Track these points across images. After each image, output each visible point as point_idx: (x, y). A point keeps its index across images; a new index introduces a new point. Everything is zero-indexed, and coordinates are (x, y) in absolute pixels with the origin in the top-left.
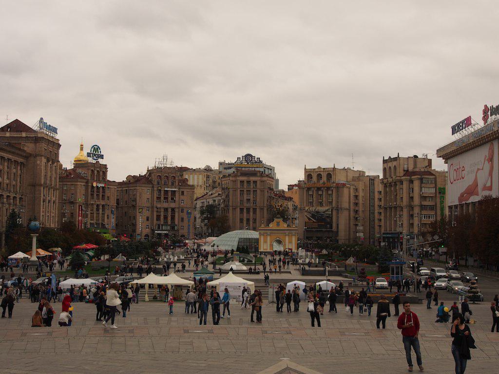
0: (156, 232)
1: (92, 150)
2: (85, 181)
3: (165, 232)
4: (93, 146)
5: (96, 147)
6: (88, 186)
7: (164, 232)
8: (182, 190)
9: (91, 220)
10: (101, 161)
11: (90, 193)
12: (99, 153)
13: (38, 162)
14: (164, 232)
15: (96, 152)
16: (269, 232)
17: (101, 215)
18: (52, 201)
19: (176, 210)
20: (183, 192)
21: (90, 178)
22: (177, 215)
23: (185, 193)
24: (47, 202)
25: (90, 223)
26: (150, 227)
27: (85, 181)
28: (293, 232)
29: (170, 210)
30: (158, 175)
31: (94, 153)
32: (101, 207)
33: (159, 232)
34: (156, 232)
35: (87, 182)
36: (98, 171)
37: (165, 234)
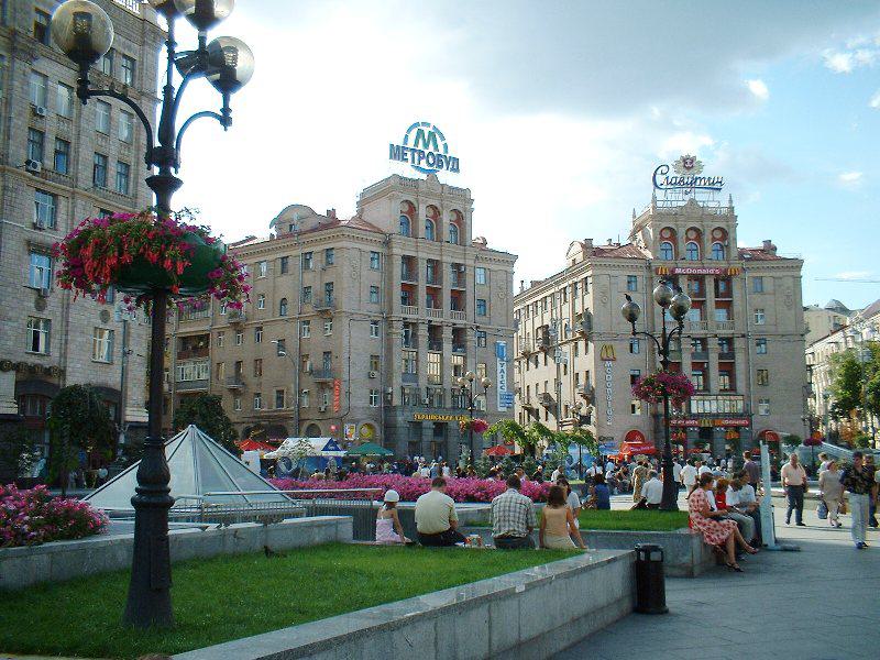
1: (414, 133)
2: (379, 237)
4: (416, 125)
5: (426, 131)
6: (390, 256)
10: (445, 177)
11: (398, 281)
12: (441, 152)
15: (425, 145)
19: (738, 344)
21: (397, 228)
22: (740, 359)
23: (768, 285)
27: (379, 237)
29: (713, 344)
30: (664, 225)
31: (420, 147)
32: (447, 334)
35: (387, 243)
36: (434, 207)
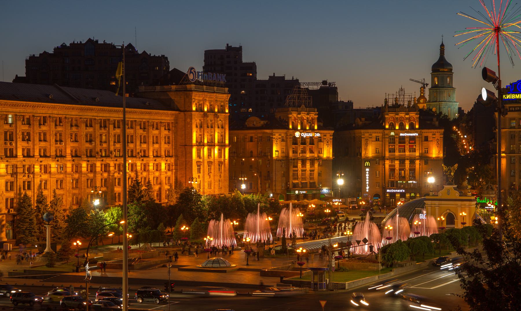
0: (388, 191)
3: (401, 191)
7: (398, 191)
8: (425, 135)
9: (295, 179)
13: (189, 120)
14: (398, 191)
16: (437, 202)
17: (308, 173)
18: (216, 163)
20: (426, 139)
24: (206, 164)
25: (293, 184)
26: (381, 184)
28: (467, 203)
33: (392, 191)
34: (388, 191)
37: (400, 193)
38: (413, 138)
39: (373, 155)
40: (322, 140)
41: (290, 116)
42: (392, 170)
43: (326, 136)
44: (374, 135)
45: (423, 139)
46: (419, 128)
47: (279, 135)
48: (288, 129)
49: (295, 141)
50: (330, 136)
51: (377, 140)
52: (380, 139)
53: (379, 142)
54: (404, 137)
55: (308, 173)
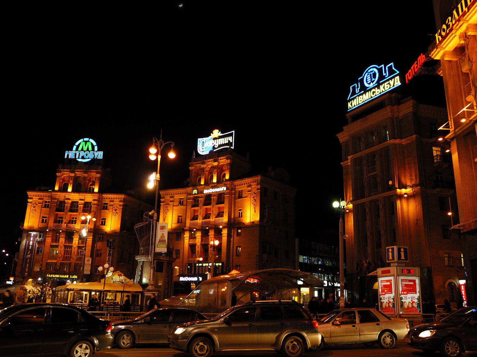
8: (239, 189)
38: (220, 197)
39: (174, 226)
40: (109, 207)
41: (58, 174)
42: (192, 247)
43: (113, 201)
44: (177, 197)
45: (237, 195)
46: (231, 179)
47: (40, 199)
48: (54, 190)
49: (61, 206)
50: (120, 201)
51: (181, 203)
52: (185, 203)
53: (182, 207)
54: (209, 196)
55: (75, 250)
